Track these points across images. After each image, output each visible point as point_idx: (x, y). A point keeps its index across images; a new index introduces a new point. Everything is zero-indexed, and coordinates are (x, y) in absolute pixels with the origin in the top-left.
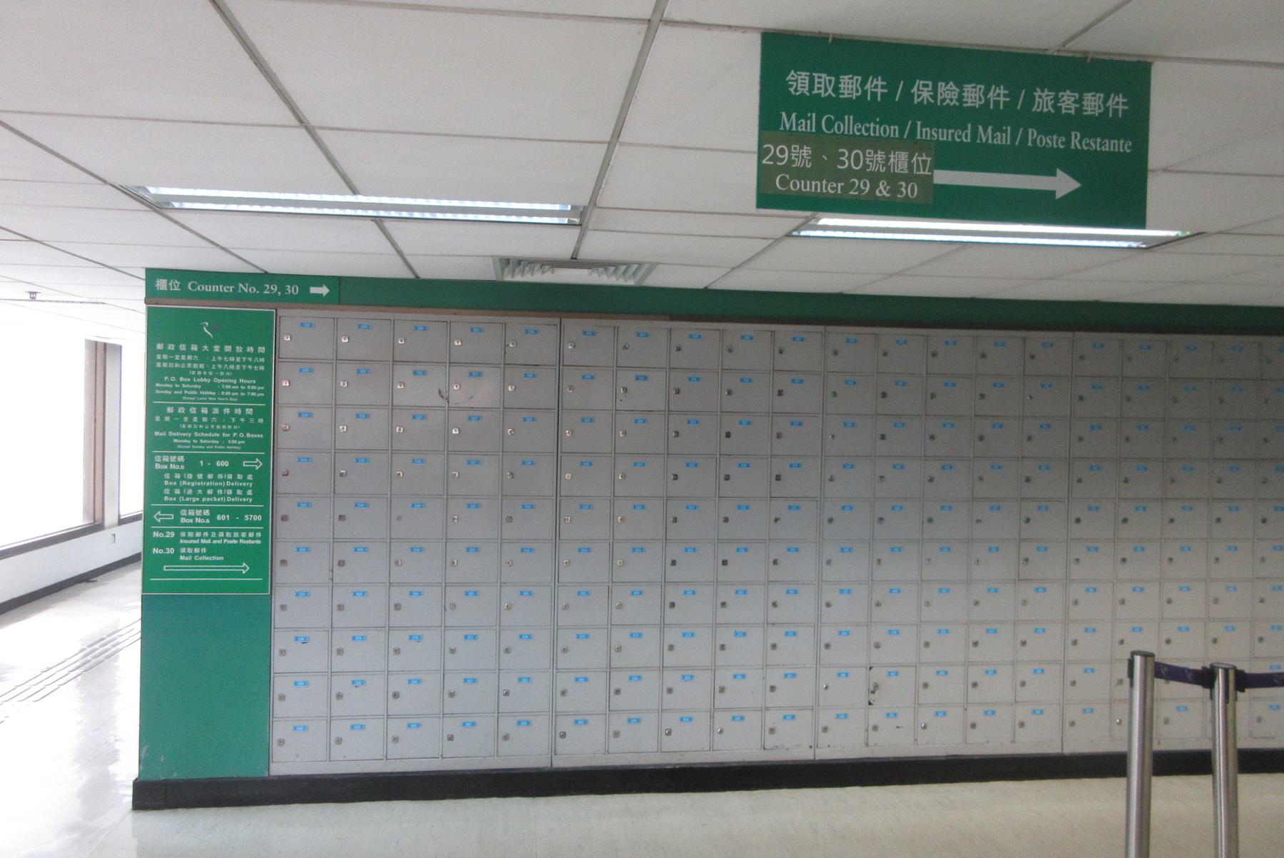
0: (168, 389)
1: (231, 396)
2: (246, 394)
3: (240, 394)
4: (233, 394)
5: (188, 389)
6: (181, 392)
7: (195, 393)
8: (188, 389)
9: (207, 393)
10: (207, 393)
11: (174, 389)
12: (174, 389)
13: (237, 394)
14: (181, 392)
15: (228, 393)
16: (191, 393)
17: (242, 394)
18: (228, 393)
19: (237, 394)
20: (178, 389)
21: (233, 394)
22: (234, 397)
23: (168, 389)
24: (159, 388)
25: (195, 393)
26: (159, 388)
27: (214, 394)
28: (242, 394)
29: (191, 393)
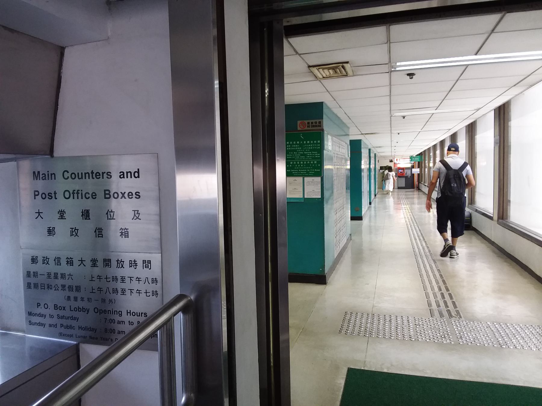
5: (297, 156)
6: (294, 157)
7: (298, 157)
8: (297, 156)
9: (302, 157)
10: (302, 157)
12: (292, 156)
14: (294, 157)
15: (309, 157)
17: (313, 157)
18: (309, 157)
20: (293, 156)
22: (310, 158)
24: (288, 156)
25: (298, 157)
26: (288, 156)
27: (304, 157)
28: (313, 157)
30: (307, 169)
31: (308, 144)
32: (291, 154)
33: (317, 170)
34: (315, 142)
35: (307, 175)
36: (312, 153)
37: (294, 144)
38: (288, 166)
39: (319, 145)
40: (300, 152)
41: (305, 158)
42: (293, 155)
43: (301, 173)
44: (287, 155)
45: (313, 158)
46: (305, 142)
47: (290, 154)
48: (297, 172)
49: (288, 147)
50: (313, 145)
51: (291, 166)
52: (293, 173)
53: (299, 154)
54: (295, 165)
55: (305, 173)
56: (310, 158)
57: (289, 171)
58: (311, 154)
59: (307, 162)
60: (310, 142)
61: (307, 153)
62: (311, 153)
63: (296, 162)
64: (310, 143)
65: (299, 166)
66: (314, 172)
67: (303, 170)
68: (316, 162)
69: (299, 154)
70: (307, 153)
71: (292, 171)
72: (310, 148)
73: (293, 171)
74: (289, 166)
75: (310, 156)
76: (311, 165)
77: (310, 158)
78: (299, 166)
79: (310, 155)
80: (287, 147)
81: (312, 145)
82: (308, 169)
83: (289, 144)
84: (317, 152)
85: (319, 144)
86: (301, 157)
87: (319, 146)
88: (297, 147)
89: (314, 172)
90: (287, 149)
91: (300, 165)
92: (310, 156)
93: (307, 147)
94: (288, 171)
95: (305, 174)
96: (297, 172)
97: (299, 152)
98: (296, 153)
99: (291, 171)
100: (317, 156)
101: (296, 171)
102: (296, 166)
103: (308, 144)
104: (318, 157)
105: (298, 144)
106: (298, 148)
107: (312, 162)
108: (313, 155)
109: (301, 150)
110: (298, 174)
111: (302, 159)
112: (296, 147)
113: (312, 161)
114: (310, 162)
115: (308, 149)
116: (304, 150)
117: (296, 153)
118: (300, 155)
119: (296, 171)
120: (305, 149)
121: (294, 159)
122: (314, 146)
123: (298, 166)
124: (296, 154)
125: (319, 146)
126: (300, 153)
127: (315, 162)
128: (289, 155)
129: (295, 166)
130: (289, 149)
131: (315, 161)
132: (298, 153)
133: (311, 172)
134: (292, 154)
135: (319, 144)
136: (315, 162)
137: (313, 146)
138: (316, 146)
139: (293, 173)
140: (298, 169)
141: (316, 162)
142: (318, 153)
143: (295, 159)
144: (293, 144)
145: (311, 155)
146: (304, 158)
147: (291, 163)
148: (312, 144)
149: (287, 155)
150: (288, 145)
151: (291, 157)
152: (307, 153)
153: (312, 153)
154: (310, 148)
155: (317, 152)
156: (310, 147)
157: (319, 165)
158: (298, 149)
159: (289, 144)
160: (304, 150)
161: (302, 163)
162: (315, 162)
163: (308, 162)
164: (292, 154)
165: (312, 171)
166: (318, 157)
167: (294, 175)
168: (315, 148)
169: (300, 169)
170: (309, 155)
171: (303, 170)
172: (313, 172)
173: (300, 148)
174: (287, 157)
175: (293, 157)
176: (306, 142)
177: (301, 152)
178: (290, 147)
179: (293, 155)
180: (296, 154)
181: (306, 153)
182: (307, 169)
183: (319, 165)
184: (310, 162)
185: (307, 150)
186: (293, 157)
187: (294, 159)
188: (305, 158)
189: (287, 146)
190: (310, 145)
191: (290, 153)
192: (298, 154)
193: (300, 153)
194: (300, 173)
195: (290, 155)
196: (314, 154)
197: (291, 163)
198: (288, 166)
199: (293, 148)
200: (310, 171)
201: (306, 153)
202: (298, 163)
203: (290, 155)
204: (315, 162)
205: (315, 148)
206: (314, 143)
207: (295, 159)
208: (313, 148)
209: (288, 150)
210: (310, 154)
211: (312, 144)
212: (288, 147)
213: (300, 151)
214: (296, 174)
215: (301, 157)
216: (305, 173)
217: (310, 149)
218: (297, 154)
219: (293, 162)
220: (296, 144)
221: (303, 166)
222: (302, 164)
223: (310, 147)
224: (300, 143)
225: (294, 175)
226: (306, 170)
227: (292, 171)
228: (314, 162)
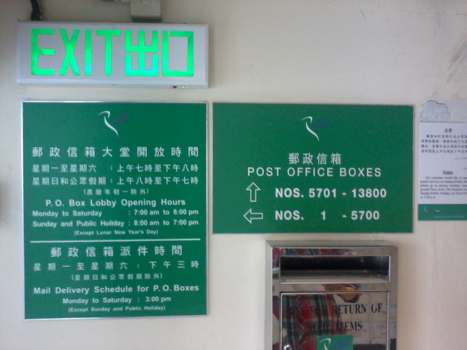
0: (51, 219)
1: (149, 227)
2: (172, 222)
3: (161, 223)
4: (152, 223)
5: (83, 219)
6: (71, 224)
7: (92, 224)
8: (83, 219)
9: (111, 223)
10: (111, 223)
11: (61, 219)
12: (61, 219)
13: (157, 223)
14: (71, 224)
15: (144, 223)
16: (86, 224)
17: (166, 223)
18: (144, 223)
19: (157, 223)
20: (67, 219)
21: (152, 223)
23: (51, 219)
24: (40, 219)
25: (92, 224)
26: (40, 219)
28: (166, 223)
29: (86, 224)
30: (134, 283)
31: (143, 161)
32: (54, 208)
33: (182, 289)
34: (176, 151)
35: (133, 308)
36: (159, 203)
37: (69, 161)
38: (37, 267)
39: (195, 168)
40: (99, 198)
41: (125, 228)
42: (65, 214)
43: (105, 300)
44: (35, 213)
45: (164, 232)
46: (125, 152)
47: (47, 209)
48: (82, 296)
49: (41, 175)
50: (163, 168)
51: (52, 267)
52: (65, 301)
53: (97, 209)
54: (74, 261)
55: (123, 300)
56: (149, 232)
57: (46, 291)
58: (154, 209)
59: (134, 247)
60: (151, 152)
61: (135, 203)
62: (154, 204)
63: (82, 248)
64: (151, 159)
65: (95, 266)
66: (169, 299)
67: (118, 289)
68: (180, 247)
69: (97, 209)
70: (133, 207)
71: (59, 290)
72: (149, 180)
73: (63, 291)
74: (44, 266)
75: (149, 218)
76: (153, 263)
77: (149, 232)
78: (95, 266)
79: (152, 213)
80: (36, 175)
81: (158, 168)
82: (143, 283)
83: (45, 159)
84: (183, 203)
85: (192, 160)
86: (103, 223)
87: (193, 174)
88: (88, 175)
89: (169, 299)
90: (36, 181)
91: (102, 266)
92: (149, 218)
93: (134, 174)
94: (37, 291)
95: (125, 305)
96: (82, 296)
97: (96, 198)
98: (78, 204)
99: (53, 290)
100: (183, 222)
101: (78, 291)
102: (80, 266)
103: (143, 161)
104: (191, 223)
105: (88, 161)
106: (92, 181)
107: (160, 250)
108: (166, 212)
109: (102, 187)
110: (90, 305)
111: (109, 233)
112: (78, 175)
113: (159, 244)
114: (150, 247)
115: (138, 187)
116: (121, 188)
117: (78, 204)
118: (100, 214)
119: (78, 291)
120: (127, 186)
121: (67, 233)
122: (172, 173)
123: (88, 266)
124: (79, 209)
125: (193, 174)
126: (102, 203)
127: (174, 247)
128: (42, 214)
129: (76, 266)
130: (46, 181)
131: (176, 243)
132: (87, 203)
133: (155, 299)
134: (59, 210)
135: (192, 160)
136: (177, 250)
137: (163, 174)
138: (180, 174)
139: (65, 301)
140: (90, 284)
141: (180, 247)
142: (188, 207)
143: (77, 233)
144: (64, 159)
145: (157, 212)
146: (118, 228)
147: (55, 252)
148: (159, 161)
149: (35, 213)
150: (39, 161)
151: (54, 225)
152: (135, 203)
153: (159, 207)
154: (149, 180)
155: (183, 203)
156: (153, 175)
157: (195, 264)
158: (88, 186)
159: (45, 159)
160: (121, 188)
161: (109, 252)
162: (174, 247)
163: (143, 250)
164: (59, 210)
165: (161, 294)
166: (191, 223)
167: (71, 310)
168: (176, 180)
169: (101, 284)
170: (144, 212)
171: (118, 289)
172: (163, 300)
173: (102, 181)
174: (35, 224)
175: (63, 224)
176: (133, 152)
177: (104, 197)
178: (51, 174)
179: (65, 214)
180: (79, 209)
181: (130, 203)
182: (134, 283)
183: (195, 264)
184: (150, 247)
185: (134, 192)
186: (63, 224)
187: (67, 233)
188: (125, 228)
189: (36, 168)
190: (148, 168)
191: (48, 202)
192: (91, 209)
193: (102, 203)
194: (101, 304)
195: (50, 214)
196: (170, 208)
197: (55, 252)
198: (37, 267)
199: (63, 181)
200: (151, 293)
201: (130, 203)
202: (91, 252)
203: (50, 214)
204: (177, 250)
205: (176, 180)
206: (168, 158)
207: (77, 233)
208: (167, 179)
209: (41, 187)
210: (149, 208)
211: (159, 161)
212: (41, 175)
213: (99, 192)
214: (82, 306)
215: (103, 223)
216: (123, 300)
217: (152, 187)
218: (88, 208)
219: (65, 248)
220: (81, 159)
221: (116, 270)
222: (109, 259)
223: (153, 175)
224: (99, 152)
225: (71, 310)
226: (130, 290)
227: (59, 290)
228: (168, 246)
